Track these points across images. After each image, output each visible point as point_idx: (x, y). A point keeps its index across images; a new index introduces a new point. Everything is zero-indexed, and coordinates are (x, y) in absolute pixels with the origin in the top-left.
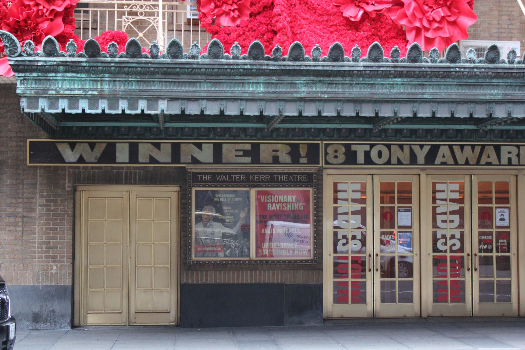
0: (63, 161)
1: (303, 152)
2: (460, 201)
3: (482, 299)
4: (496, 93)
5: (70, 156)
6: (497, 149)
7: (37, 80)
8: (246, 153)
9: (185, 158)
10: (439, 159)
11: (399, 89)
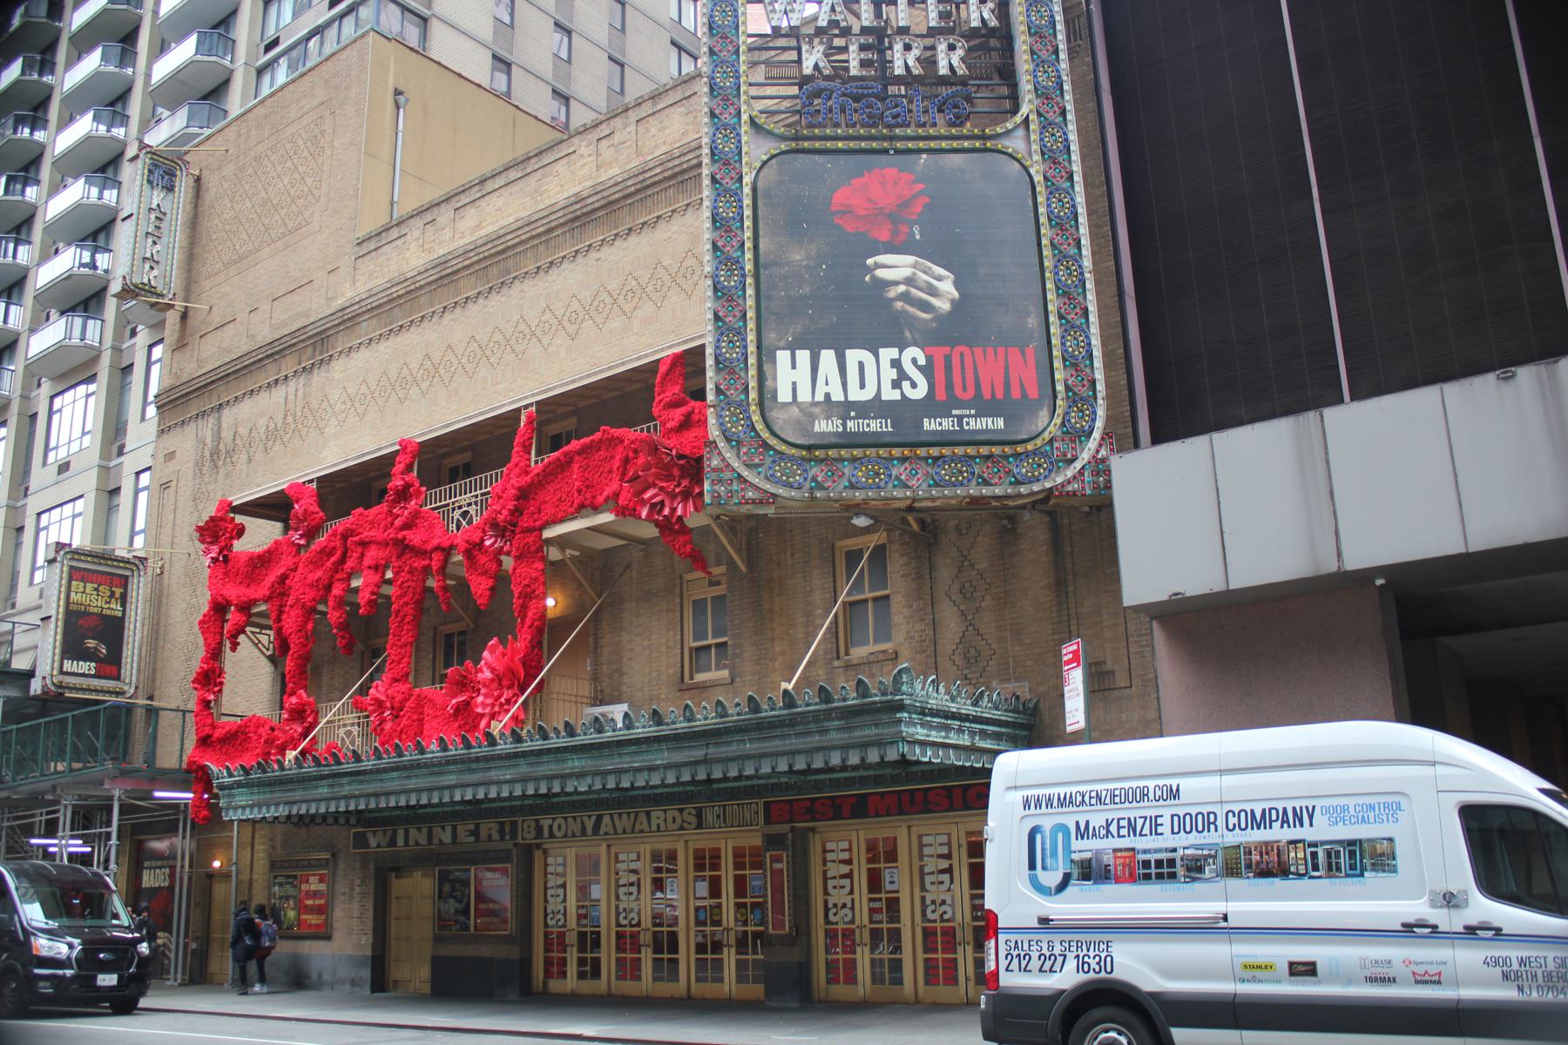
0: (368, 846)
1: (507, 829)
2: (849, 862)
3: (655, 979)
4: (451, 779)
5: (373, 842)
6: (648, 814)
7: (229, 796)
8: (472, 833)
9: (436, 841)
10: (602, 831)
11: (393, 782)
